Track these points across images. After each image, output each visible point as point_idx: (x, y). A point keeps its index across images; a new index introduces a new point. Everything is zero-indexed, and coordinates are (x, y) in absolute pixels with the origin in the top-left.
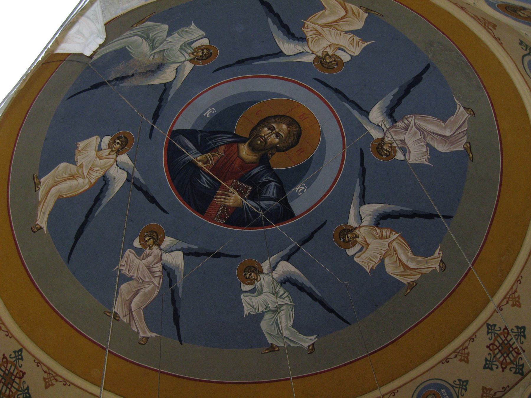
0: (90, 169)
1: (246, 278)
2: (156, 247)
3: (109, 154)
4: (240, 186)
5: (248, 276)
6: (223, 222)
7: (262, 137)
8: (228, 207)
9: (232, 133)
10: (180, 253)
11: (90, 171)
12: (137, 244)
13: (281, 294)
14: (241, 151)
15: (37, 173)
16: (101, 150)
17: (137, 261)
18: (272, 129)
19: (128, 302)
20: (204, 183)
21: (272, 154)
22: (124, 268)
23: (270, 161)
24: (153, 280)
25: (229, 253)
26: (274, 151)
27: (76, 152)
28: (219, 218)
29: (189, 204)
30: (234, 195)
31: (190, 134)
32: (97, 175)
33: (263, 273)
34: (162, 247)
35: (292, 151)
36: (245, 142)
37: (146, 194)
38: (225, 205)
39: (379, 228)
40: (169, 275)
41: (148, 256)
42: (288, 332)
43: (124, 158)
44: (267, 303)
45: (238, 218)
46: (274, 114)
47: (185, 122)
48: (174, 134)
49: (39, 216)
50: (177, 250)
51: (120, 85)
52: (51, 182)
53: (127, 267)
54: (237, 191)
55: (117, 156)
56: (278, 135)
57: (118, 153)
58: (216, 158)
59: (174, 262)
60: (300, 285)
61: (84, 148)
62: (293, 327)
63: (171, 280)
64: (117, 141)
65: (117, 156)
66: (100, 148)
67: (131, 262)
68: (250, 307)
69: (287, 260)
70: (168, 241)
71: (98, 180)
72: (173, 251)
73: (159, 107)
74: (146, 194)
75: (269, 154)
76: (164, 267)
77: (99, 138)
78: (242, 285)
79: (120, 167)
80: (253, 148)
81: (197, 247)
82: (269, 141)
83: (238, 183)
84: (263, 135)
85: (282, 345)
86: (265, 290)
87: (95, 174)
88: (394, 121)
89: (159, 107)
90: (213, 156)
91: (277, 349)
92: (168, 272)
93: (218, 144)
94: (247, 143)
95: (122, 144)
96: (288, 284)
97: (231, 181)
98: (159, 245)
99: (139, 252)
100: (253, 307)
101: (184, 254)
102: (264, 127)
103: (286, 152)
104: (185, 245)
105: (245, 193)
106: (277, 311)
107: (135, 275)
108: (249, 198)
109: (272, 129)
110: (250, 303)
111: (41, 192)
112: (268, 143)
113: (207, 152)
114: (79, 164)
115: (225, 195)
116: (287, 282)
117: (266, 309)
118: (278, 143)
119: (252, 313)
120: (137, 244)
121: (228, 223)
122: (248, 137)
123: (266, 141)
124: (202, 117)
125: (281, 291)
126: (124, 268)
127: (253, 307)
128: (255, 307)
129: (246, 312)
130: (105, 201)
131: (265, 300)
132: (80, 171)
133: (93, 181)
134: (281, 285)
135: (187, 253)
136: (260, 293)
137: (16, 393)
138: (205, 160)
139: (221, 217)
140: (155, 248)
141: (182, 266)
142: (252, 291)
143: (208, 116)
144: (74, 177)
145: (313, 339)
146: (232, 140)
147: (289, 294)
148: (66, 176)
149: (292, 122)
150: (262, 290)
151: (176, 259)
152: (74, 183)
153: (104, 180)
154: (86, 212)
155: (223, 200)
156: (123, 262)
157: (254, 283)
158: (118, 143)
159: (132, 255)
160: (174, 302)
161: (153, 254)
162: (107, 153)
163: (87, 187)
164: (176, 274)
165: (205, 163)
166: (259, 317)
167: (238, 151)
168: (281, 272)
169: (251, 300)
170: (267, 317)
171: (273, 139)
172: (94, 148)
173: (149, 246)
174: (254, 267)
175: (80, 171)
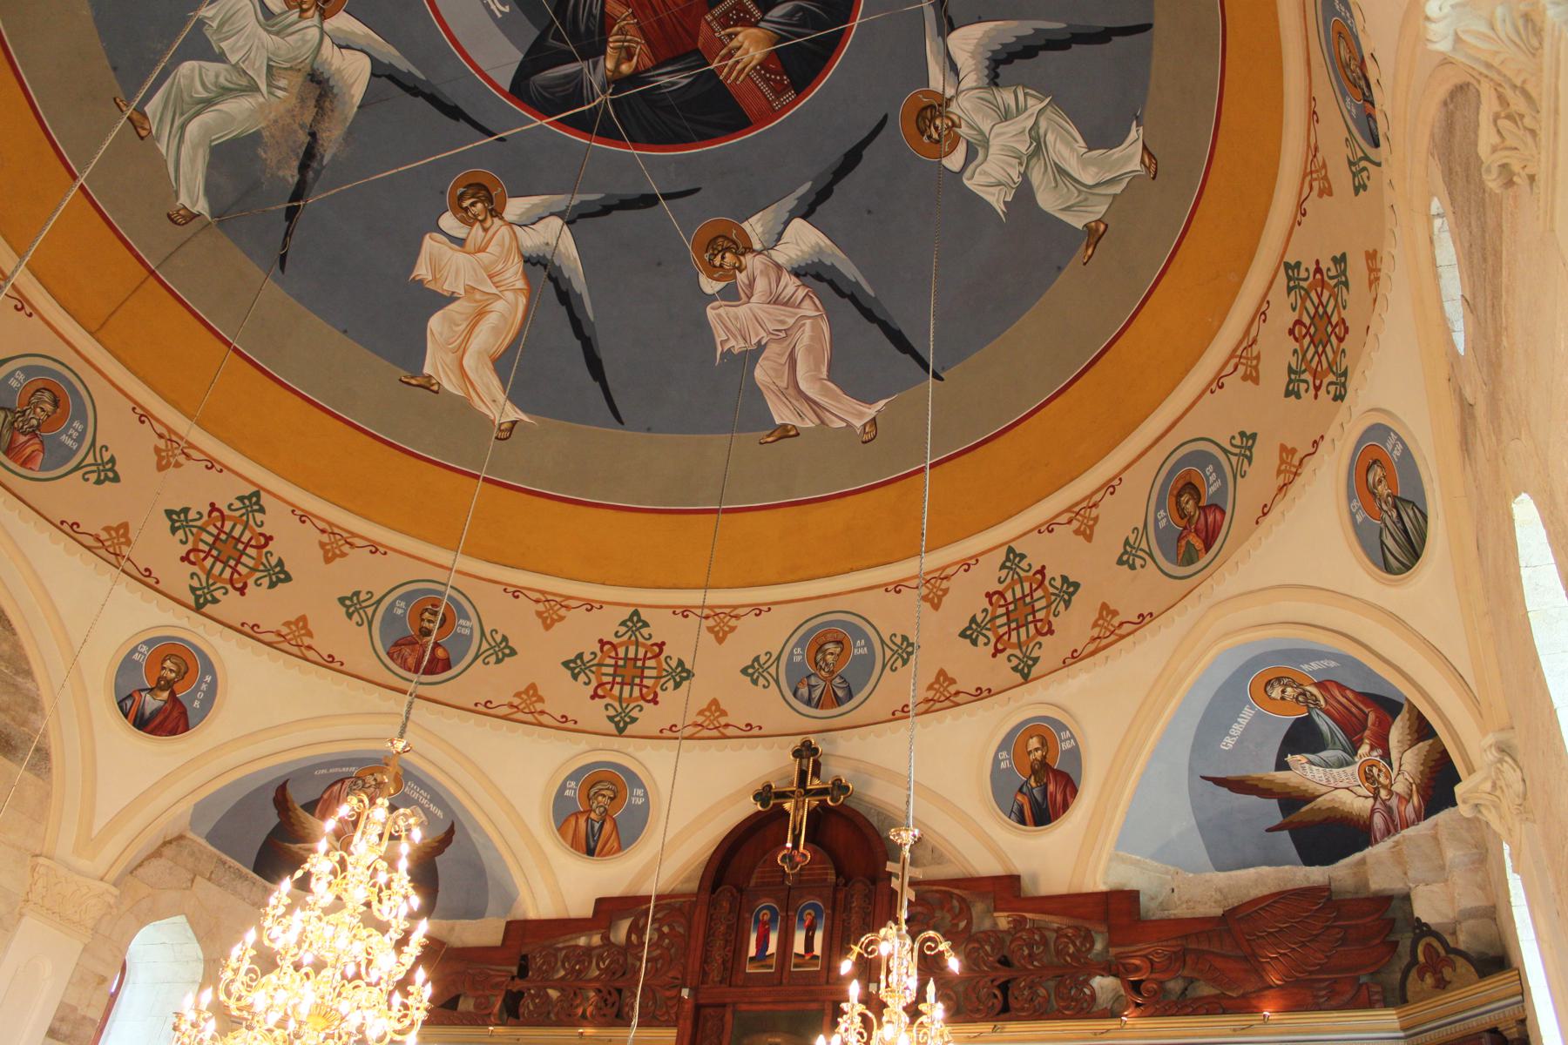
0: (491, 277)
1: (938, 142)
2: (749, 257)
3: (486, 230)
4: (725, 14)
5: (935, 136)
6: (791, 95)
8: (763, 64)
10: (798, 223)
11: (496, 279)
12: (709, 286)
13: (1013, 104)
15: (403, 374)
16: (464, 240)
17: (742, 311)
19: (791, 391)
20: (673, 84)
22: (732, 343)
24: (802, 312)
25: (865, 134)
27: (431, 286)
28: (778, 98)
29: (705, 138)
30: (740, 37)
31: (536, 59)
32: (513, 273)
33: (950, 100)
34: (757, 246)
37: (626, 204)
38: (754, 68)
40: (818, 277)
41: (751, 285)
42: (1093, 170)
44: (1014, 150)
45: (798, 65)
48: (520, 89)
49: (484, 410)
50: (786, 223)
51: (325, 162)
52: (450, 358)
53: (735, 337)
54: (735, 25)
55: (502, 219)
57: (496, 213)
58: (632, 30)
59: (805, 248)
60: (1019, 48)
62: (1090, 149)
63: (832, 284)
64: (466, 203)
65: (502, 219)
66: (460, 242)
67: (729, 326)
68: (995, 190)
69: (952, 28)
70: (755, 227)
71: (526, 276)
72: (780, 235)
73: (434, 100)
74: (626, 204)
76: (797, 273)
77: (436, 235)
78: (945, 162)
81: (808, 185)
83: (717, 11)
85: (1103, 209)
86: (986, 128)
87: (508, 274)
89: (434, 100)
90: (622, 31)
91: (1102, 227)
92: (812, 273)
93: (596, 11)
95: (483, 198)
96: (1001, 69)
97: (703, 26)
98: (749, 249)
99: (730, 295)
100: (999, 184)
101: (804, 217)
104: (790, 202)
105: (747, 11)
106: (1039, 144)
107: (763, 334)
108: (764, 12)
110: (990, 181)
111: (450, 385)
113: (606, 42)
115: (730, 55)
116: (1001, 64)
117: (1021, 164)
119: (1009, 199)
120: (709, 286)
121: (801, 85)
124: (503, 24)
125: (1006, 96)
126: (732, 343)
127: (999, 184)
128: (1004, 179)
129: (1000, 208)
130: (579, 284)
131: (1005, 148)
132: (478, 296)
133: (520, 284)
134: (996, 85)
135: (807, 211)
136: (986, 144)
137: (655, 685)
138: (624, 54)
139: (779, 91)
140: (748, 260)
141: (824, 241)
142: (971, 155)
143: (507, 9)
144: (481, 314)
145: (1135, 133)
147: (1024, 86)
150: (981, 132)
151: (803, 240)
153: (534, 265)
154: (568, 331)
155: (739, 67)
156: (720, 335)
157: (958, 138)
158: (473, 204)
159: (721, 311)
160: (869, 315)
161: (757, 272)
162: (480, 231)
163: (522, 301)
164: (828, 263)
165: (630, 58)
166: (1024, 192)
168: (971, 62)
169: (985, 173)
170: (1036, 177)
172: (450, 252)
173: (735, 268)
174: (925, 108)
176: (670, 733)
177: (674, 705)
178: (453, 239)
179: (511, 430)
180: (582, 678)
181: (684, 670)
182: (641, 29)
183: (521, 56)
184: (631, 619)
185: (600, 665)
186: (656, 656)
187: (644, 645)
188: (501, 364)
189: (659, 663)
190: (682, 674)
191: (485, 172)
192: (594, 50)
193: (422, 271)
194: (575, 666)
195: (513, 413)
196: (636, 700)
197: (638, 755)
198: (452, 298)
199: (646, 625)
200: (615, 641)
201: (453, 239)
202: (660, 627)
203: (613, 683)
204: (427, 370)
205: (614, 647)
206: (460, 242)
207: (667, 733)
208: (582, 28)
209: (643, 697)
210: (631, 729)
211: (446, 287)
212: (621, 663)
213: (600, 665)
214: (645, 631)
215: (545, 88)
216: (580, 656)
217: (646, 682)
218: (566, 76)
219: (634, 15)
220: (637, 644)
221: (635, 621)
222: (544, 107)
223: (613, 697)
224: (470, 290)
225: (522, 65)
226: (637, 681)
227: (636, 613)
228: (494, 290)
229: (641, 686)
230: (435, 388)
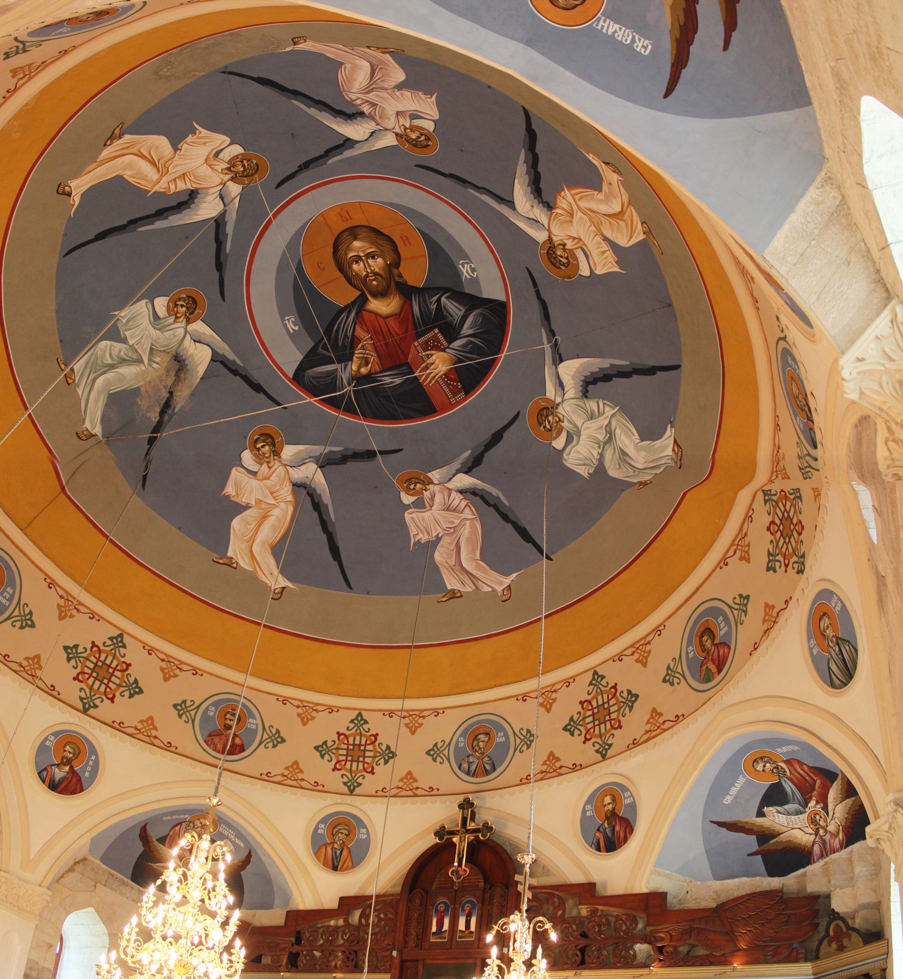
0: (272, 493)
7: (367, 276)
9: (342, 311)
11: (275, 495)
14: (379, 311)
18: (358, 259)
21: (400, 276)
23: (409, 284)
26: (395, 271)
31: (311, 360)
32: (286, 492)
35: (403, 250)
36: (367, 299)
39: (555, 208)
43: (289, 451)
46: (330, 249)
47: (289, 358)
48: (299, 377)
52: (244, 546)
56: (372, 256)
58: (369, 347)
61: (237, 488)
66: (254, 474)
75: (397, 279)
79: (299, 463)
80: (381, 294)
82: (377, 270)
84: (364, 273)
88: (361, 114)
90: (363, 348)
93: (349, 334)
94: (369, 297)
102: (350, 267)
103: (402, 257)
109: (358, 259)
111: (244, 563)
112: (381, 272)
113: (353, 353)
114: (254, 503)
118: (385, 261)
122: (359, 293)
123: (376, 274)
132: (263, 506)
144: (264, 517)
146: (353, 315)
148: (253, 526)
149: (353, 232)
152: (271, 521)
167: (376, 314)
171: (377, 264)
172: (247, 479)
175: (263, 506)
176: (382, 793)
177: (385, 775)
178: (250, 472)
179: (281, 593)
180: (327, 757)
181: (391, 752)
182: (376, 348)
183: (301, 357)
184: (356, 718)
185: (338, 749)
186: (373, 743)
187: (365, 736)
188: (276, 550)
189: (375, 747)
190: (389, 755)
191: (272, 427)
192: (345, 357)
193: (230, 490)
194: (322, 749)
195: (283, 582)
196: (360, 771)
197: (363, 807)
198: (247, 507)
199: (366, 722)
200: (347, 733)
201: (250, 472)
202: (376, 724)
203: (346, 761)
204: (230, 553)
205: (347, 737)
206: (254, 474)
207: (380, 793)
208: (340, 343)
209: (365, 770)
210: (358, 790)
211: (244, 500)
212: (351, 747)
213: (338, 749)
214: (366, 727)
215: (313, 378)
216: (325, 743)
217: (367, 760)
218: (327, 372)
219: (371, 338)
220: (361, 735)
221: (359, 720)
222: (313, 390)
223: (346, 770)
224: (259, 502)
225: (302, 363)
226: (361, 759)
227: (360, 714)
228: (273, 502)
229: (364, 762)
230: (235, 565)
